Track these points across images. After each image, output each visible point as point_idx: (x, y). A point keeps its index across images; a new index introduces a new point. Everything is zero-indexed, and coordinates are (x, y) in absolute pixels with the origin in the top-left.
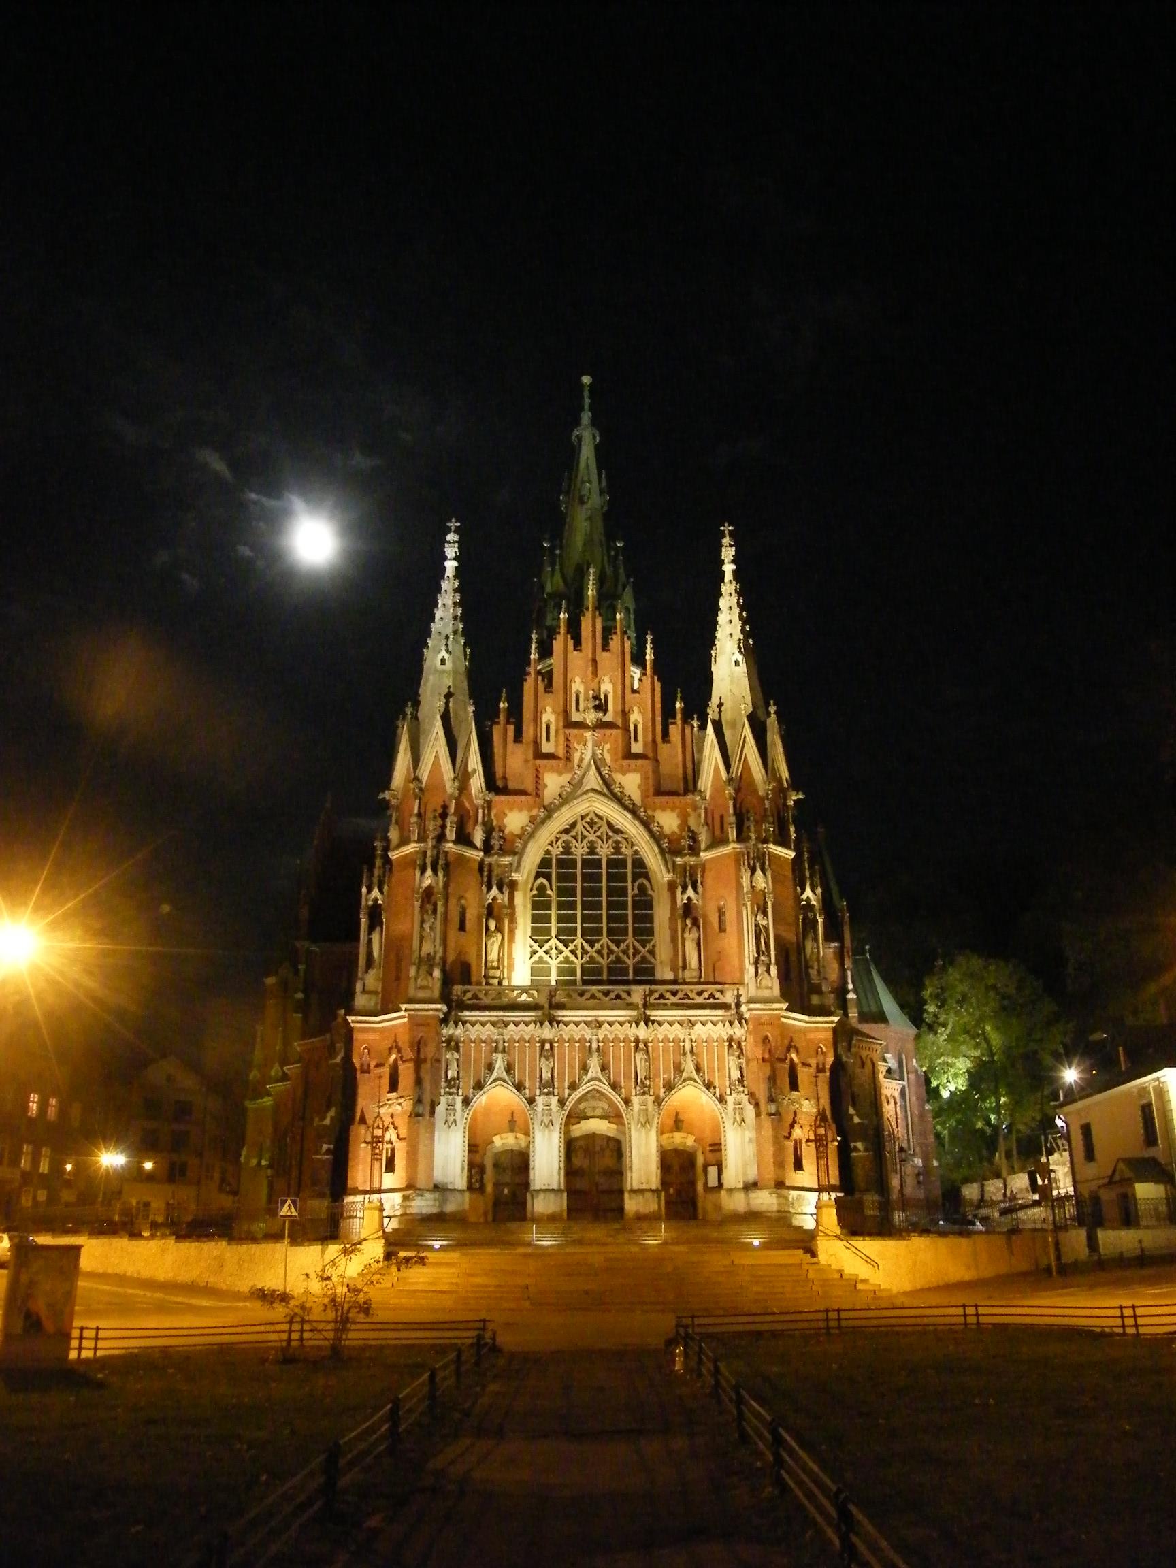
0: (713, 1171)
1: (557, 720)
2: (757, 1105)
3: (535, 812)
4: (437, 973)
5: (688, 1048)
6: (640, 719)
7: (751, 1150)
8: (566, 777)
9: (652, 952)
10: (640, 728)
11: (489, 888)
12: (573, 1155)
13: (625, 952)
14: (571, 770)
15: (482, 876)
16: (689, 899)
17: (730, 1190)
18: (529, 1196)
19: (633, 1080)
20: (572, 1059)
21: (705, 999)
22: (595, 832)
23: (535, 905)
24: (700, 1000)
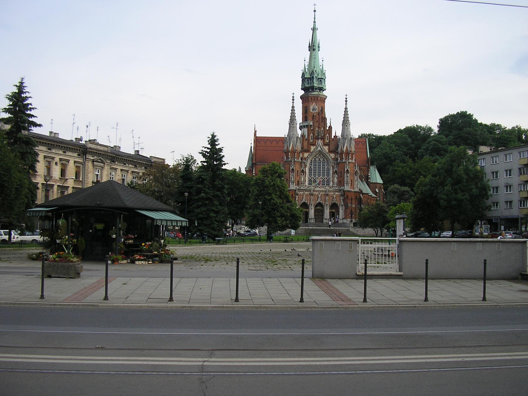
0: (338, 216)
1: (313, 136)
2: (345, 207)
3: (309, 153)
4: (294, 184)
7: (344, 213)
8: (315, 147)
9: (329, 178)
11: (302, 167)
13: (325, 178)
14: (316, 146)
15: (300, 165)
17: (340, 219)
20: (316, 198)
23: (309, 170)
24: (337, 188)
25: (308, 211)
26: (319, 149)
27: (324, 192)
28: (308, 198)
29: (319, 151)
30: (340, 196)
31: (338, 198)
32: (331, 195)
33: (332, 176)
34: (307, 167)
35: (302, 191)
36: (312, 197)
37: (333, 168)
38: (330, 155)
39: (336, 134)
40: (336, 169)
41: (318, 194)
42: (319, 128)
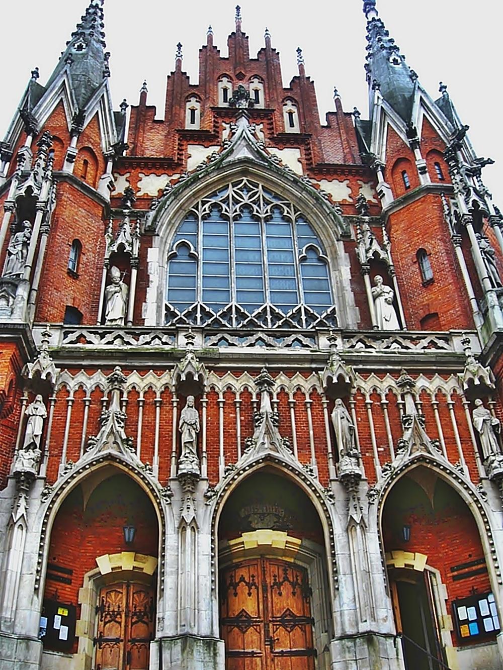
5: (411, 410)
6: (294, 109)
9: (332, 317)
10: (295, 116)
12: (231, 591)
16: (376, 253)
18: (154, 647)
19: (331, 456)
20: (230, 423)
21: (424, 348)
22: (250, 197)
24: (416, 349)
25: (148, 569)
26: (243, 153)
27: (306, 373)
28: (149, 427)
29: (246, 161)
30: (458, 407)
31: (447, 425)
32: (375, 395)
33: (350, 297)
34: (156, 241)
35: (90, 370)
36: (189, 414)
37: (351, 246)
38: (316, 186)
39: (338, 102)
40: (376, 246)
41: (246, 393)
42: (240, 77)
